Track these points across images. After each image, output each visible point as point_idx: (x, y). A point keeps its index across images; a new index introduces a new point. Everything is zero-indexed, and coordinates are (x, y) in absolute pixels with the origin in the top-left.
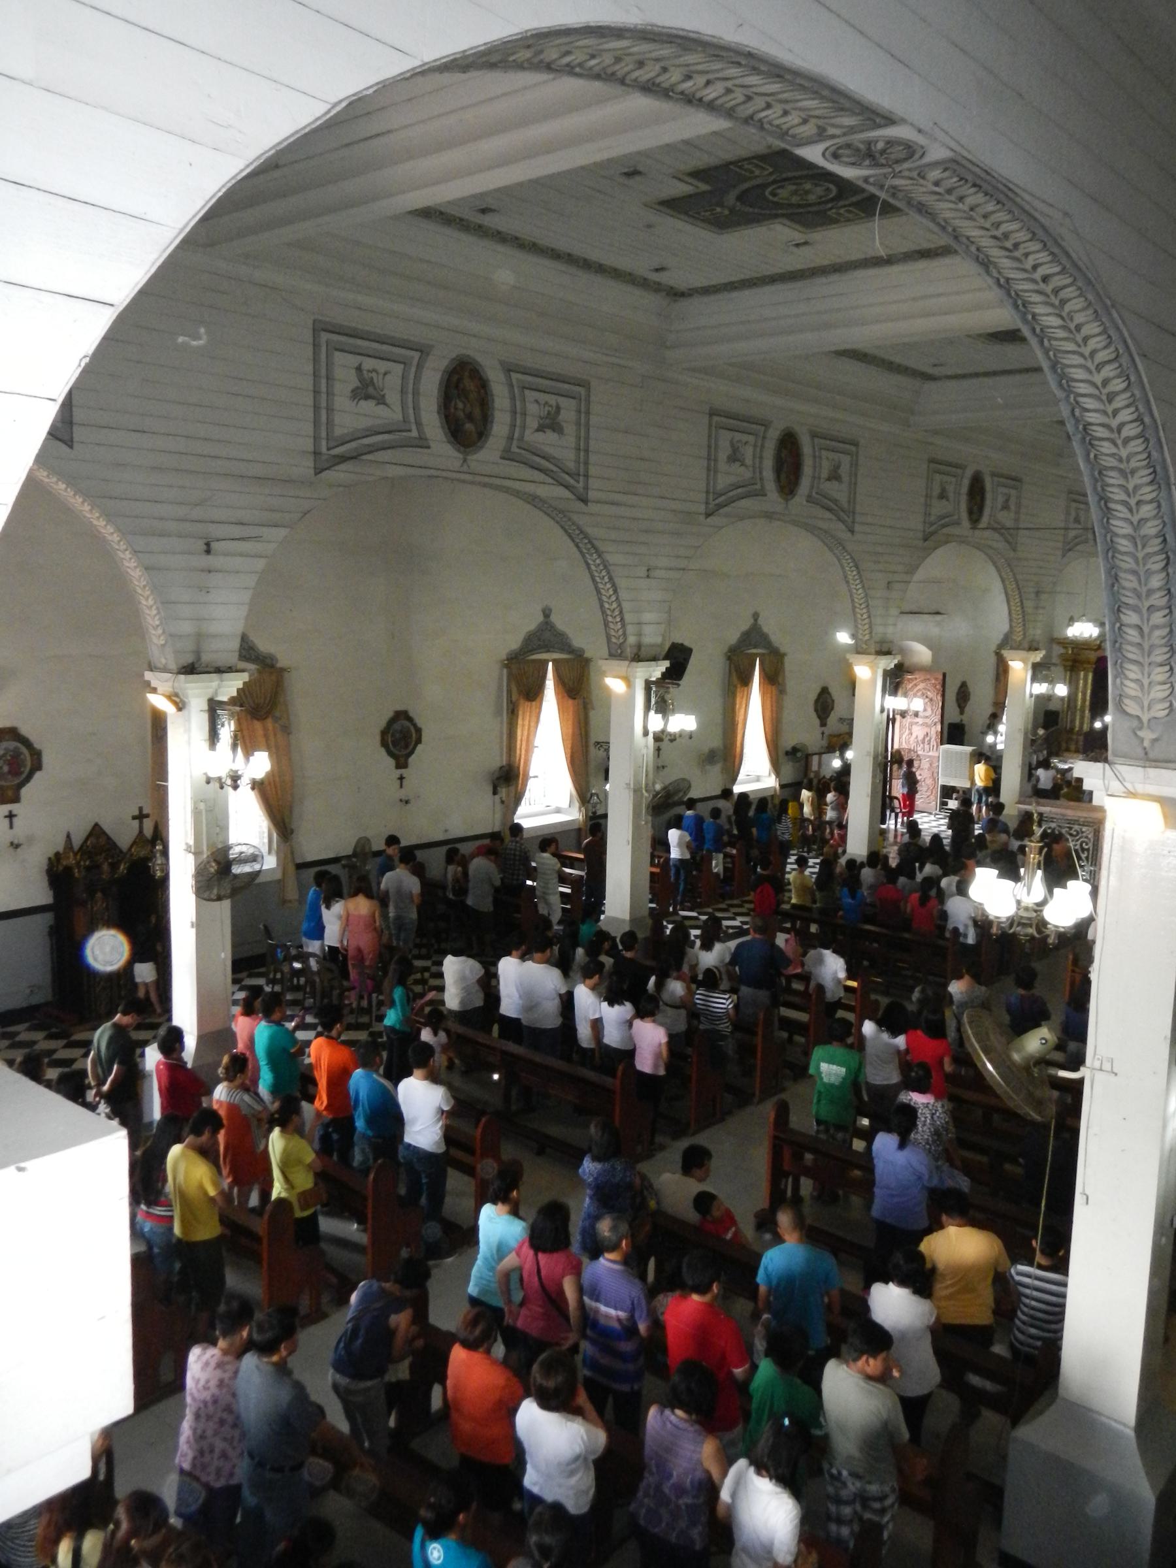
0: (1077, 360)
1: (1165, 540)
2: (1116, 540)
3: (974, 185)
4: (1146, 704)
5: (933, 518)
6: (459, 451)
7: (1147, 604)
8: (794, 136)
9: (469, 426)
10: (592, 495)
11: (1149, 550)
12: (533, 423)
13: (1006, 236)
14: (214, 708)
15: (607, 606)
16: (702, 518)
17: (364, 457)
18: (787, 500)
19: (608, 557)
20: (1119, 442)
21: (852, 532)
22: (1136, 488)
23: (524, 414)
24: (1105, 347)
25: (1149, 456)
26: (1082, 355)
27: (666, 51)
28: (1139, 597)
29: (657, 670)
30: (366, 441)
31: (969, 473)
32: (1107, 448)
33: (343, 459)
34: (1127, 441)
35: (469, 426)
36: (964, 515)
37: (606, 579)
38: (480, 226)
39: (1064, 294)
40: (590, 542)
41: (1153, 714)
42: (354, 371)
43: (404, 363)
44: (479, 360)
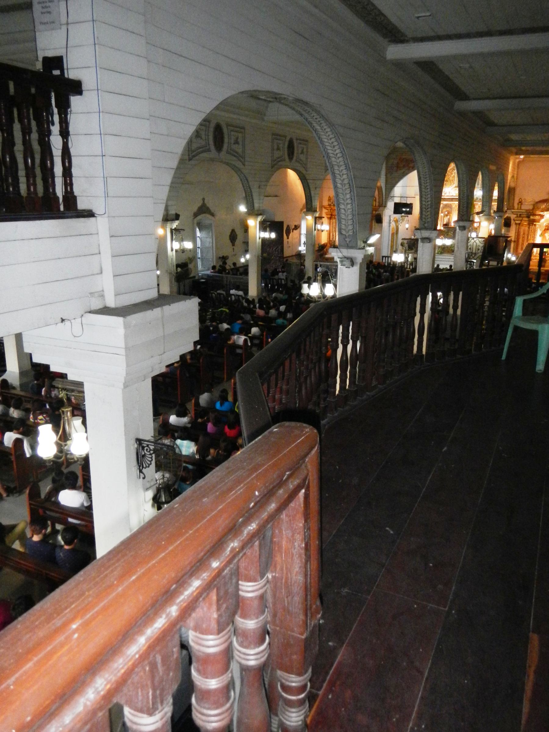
0: (325, 137)
1: (350, 185)
11: (346, 187)
16: (187, 161)
18: (219, 153)
21: (244, 165)
22: (342, 170)
26: (326, 136)
28: (344, 200)
31: (288, 139)
32: (333, 159)
34: (339, 158)
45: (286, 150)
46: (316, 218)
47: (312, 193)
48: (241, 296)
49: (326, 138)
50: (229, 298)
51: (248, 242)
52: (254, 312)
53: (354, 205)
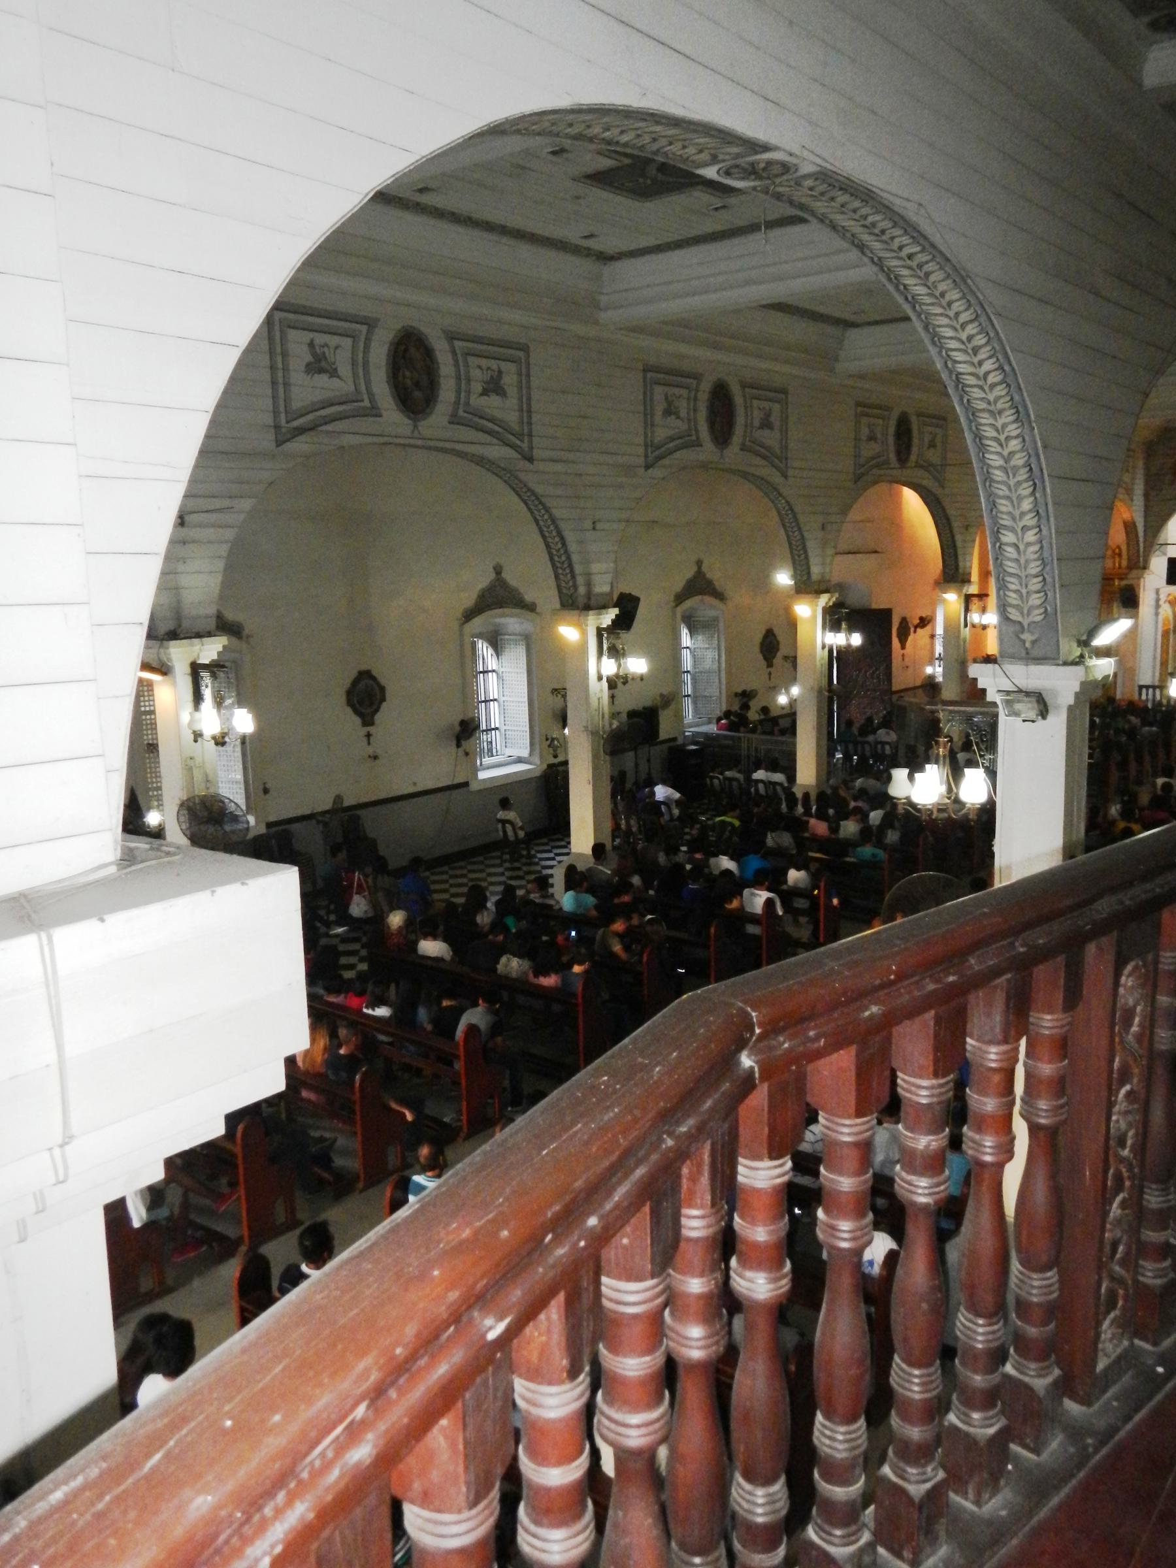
0: (945, 321)
1: (1031, 469)
2: (991, 470)
3: (841, 189)
4: (1025, 611)
5: (862, 461)
6: (409, 418)
7: (1021, 524)
8: (693, 162)
9: (417, 394)
10: (536, 453)
12: (477, 387)
13: (874, 225)
14: (196, 670)
15: (556, 558)
16: (642, 470)
17: (320, 428)
19: (557, 513)
20: (986, 388)
21: (786, 477)
22: (1004, 426)
23: (469, 380)
24: (966, 310)
25: (1012, 399)
27: (588, 117)
28: (1014, 519)
29: (608, 617)
30: (323, 413)
31: (895, 415)
32: (977, 393)
33: (301, 431)
34: (992, 386)
35: (417, 394)
36: (892, 456)
37: (554, 533)
38: (418, 204)
39: (926, 268)
40: (537, 499)
41: (1031, 619)
42: (306, 348)
43: (353, 337)
44: (422, 329)
45: (891, 440)
46: (968, 599)
47: (958, 538)
48: (781, 784)
49: (947, 326)
50: (753, 790)
51: (795, 658)
52: (804, 826)
53: (1045, 532)
